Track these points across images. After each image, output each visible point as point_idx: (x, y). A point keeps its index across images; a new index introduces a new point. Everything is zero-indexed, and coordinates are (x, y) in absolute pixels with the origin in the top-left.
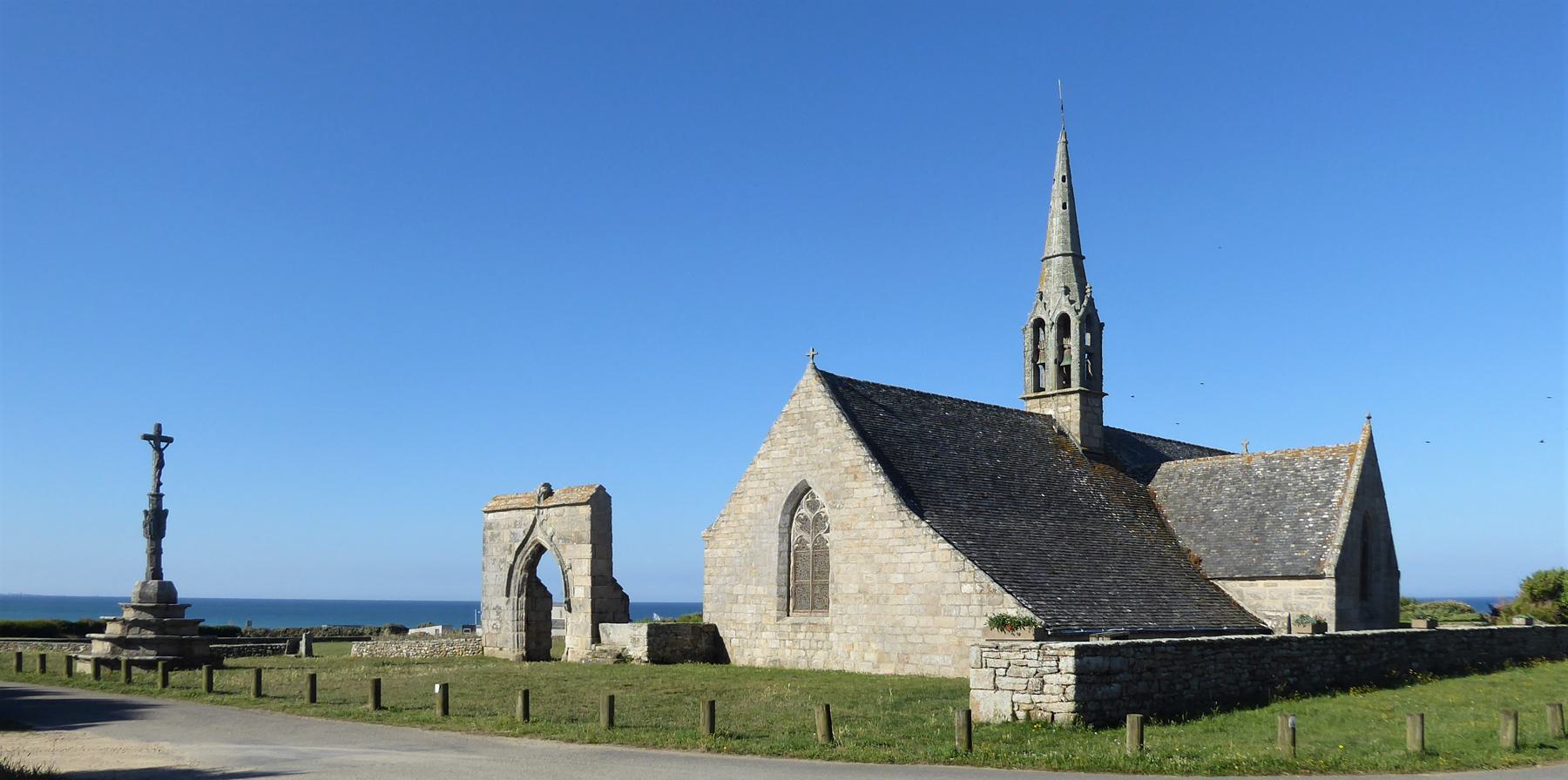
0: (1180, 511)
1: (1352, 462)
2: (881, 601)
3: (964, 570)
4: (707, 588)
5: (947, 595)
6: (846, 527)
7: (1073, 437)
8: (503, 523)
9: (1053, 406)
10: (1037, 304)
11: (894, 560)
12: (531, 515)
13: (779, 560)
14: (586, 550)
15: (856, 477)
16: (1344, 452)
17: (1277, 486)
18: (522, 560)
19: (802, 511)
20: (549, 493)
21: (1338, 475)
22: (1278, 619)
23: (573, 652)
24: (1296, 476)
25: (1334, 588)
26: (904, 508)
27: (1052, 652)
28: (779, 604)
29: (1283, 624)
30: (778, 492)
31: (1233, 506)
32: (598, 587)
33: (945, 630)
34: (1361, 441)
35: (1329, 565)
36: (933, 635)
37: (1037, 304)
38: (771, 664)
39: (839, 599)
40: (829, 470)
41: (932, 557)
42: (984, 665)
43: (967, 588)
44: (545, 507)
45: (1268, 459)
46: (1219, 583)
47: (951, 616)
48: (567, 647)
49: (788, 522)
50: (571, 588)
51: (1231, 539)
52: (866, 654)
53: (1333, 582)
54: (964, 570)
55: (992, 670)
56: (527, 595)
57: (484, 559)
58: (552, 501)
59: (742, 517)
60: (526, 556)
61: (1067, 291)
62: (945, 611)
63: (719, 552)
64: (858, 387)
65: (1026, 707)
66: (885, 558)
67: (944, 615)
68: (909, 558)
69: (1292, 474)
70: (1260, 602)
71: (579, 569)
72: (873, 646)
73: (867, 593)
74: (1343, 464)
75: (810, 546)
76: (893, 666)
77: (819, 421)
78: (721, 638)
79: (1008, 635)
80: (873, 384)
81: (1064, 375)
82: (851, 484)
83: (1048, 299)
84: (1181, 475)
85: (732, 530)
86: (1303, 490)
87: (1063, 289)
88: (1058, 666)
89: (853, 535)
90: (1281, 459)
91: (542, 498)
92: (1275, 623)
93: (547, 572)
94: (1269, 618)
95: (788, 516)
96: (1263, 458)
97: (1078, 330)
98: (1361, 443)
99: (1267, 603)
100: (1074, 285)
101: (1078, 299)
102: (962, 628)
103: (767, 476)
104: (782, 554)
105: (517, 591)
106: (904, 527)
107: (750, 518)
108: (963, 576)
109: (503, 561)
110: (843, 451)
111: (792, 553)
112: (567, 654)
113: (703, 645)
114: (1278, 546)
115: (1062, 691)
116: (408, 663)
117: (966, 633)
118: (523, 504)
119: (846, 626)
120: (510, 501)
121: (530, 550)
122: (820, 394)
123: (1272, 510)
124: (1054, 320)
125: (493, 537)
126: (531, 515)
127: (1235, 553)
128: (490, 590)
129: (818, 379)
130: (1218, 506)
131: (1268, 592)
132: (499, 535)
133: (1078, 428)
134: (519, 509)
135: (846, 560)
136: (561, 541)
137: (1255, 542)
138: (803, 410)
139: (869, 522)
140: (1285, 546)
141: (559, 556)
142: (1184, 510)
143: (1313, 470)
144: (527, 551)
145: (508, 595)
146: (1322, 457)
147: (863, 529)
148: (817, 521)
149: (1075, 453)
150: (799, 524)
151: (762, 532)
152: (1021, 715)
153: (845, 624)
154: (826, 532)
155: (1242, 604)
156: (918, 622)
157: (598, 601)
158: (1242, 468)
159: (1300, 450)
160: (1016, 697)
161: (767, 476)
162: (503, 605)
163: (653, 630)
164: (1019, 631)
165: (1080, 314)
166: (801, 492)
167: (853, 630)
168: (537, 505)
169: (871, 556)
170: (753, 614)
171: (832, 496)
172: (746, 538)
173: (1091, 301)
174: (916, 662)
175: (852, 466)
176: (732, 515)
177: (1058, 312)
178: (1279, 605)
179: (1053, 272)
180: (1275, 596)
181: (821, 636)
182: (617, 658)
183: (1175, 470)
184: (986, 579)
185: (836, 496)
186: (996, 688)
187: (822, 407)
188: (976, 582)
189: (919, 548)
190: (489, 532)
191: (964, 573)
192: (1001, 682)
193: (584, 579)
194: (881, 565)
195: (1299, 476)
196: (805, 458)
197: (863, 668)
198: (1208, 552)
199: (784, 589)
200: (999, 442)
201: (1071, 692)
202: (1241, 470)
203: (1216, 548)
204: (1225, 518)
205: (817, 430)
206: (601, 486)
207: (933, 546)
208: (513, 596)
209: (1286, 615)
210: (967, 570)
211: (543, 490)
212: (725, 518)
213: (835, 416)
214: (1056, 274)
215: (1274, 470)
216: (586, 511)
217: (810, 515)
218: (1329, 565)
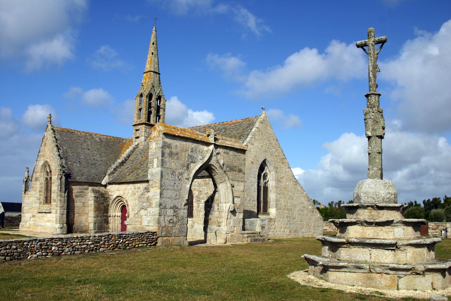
132: (177, 154)
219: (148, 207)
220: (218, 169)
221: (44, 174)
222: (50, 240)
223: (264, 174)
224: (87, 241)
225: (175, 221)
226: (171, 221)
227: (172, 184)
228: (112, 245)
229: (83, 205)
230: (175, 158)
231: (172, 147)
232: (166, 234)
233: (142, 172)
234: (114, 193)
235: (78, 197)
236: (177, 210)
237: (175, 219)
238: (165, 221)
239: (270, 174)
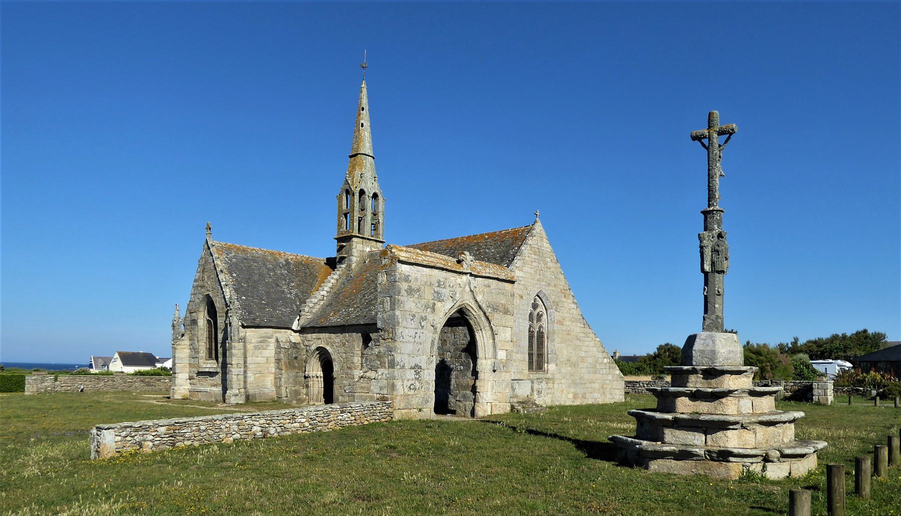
40: (553, 288)
41: (595, 344)
43: (605, 361)
66: (578, 343)
82: (564, 299)
103: (522, 283)
132: (419, 290)
134: (443, 269)
138: (540, 247)
161: (522, 283)
170: (514, 372)
177: (374, 192)
189: (590, 339)
219: (379, 368)
220: (477, 311)
221: (204, 314)
222: (250, 418)
223: (538, 315)
224: (300, 417)
225: (417, 388)
226: (412, 387)
227: (413, 335)
228: (333, 422)
229: (267, 360)
230: (416, 296)
231: (411, 281)
232: (406, 406)
233: (354, 310)
234: (313, 342)
235: (259, 349)
237: (418, 385)
238: (403, 387)
239: (547, 313)
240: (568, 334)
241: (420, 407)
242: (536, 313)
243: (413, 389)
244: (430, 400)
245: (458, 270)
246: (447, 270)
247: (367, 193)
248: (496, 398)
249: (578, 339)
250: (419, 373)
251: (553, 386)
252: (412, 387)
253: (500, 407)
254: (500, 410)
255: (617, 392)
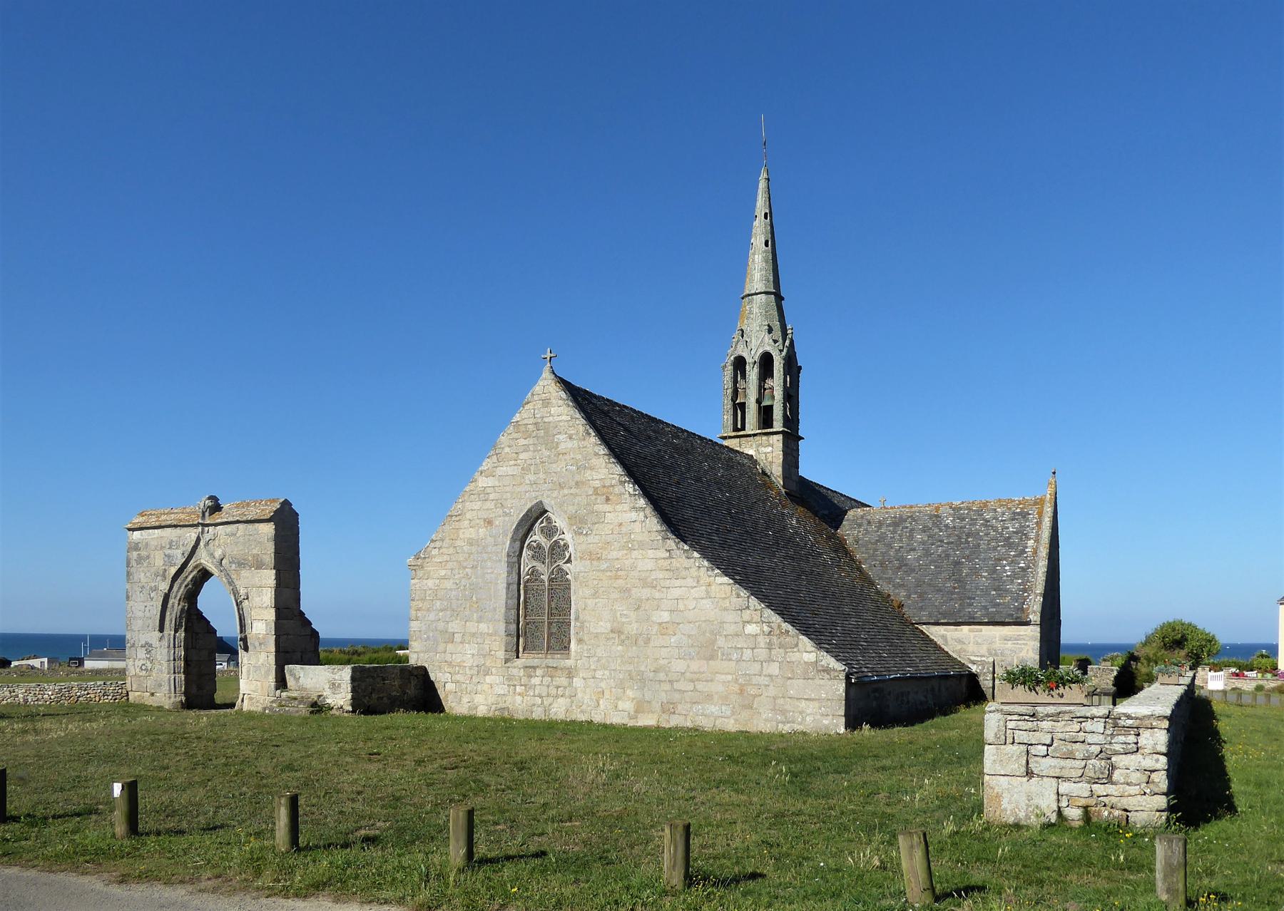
0: (873, 557)
1: (1040, 514)
2: (641, 642)
3: (748, 608)
4: (414, 625)
5: (726, 636)
6: (594, 557)
7: (775, 478)
8: (153, 543)
9: (754, 446)
10: (738, 341)
11: (657, 595)
12: (192, 534)
13: (507, 594)
14: (268, 577)
15: (608, 499)
16: (1030, 505)
17: (968, 535)
18: (180, 588)
19: (534, 538)
20: (216, 508)
21: (1028, 526)
22: (983, 663)
23: (251, 699)
24: (986, 526)
25: (1039, 635)
26: (670, 535)
27: (1130, 722)
28: (507, 644)
29: (988, 669)
30: (506, 514)
31: (927, 553)
32: (285, 622)
33: (723, 677)
34: (1050, 491)
35: (1034, 612)
36: (707, 681)
37: (738, 341)
38: (497, 713)
39: (586, 638)
40: (573, 491)
41: (707, 592)
42: (1009, 740)
43: (751, 629)
44: (211, 525)
45: (957, 509)
46: (923, 628)
47: (731, 660)
48: (241, 692)
49: (518, 550)
50: (248, 622)
51: (929, 585)
52: (620, 702)
53: (1038, 629)
54: (748, 608)
55: (1024, 748)
56: (186, 630)
57: (128, 586)
58: (218, 518)
59: (459, 543)
60: (186, 583)
61: (770, 330)
62: (723, 655)
63: (430, 583)
64: (594, 401)
65: (1083, 802)
66: (646, 593)
67: (722, 660)
68: (676, 593)
69: (982, 524)
70: (964, 646)
71: (257, 599)
72: (630, 693)
73: (622, 633)
74: (1031, 516)
75: (545, 578)
76: (656, 716)
77: (560, 433)
78: (432, 682)
79: (1043, 697)
80: (608, 400)
81: (766, 416)
82: (601, 507)
83: (750, 337)
84: (869, 522)
85: (446, 558)
86: (996, 539)
87: (767, 327)
88: (1137, 743)
89: (604, 566)
90: (969, 509)
91: (207, 514)
92: (980, 667)
93: (212, 603)
94: (974, 663)
95: (518, 544)
96: (951, 507)
97: (782, 370)
98: (1048, 496)
99: (971, 648)
100: (776, 325)
101: (780, 339)
102: (746, 674)
103: (491, 497)
104: (511, 587)
105: (173, 625)
106: (670, 557)
107: (471, 544)
108: (747, 615)
109: (155, 589)
110: (592, 469)
111: (522, 586)
112: (243, 701)
113: (412, 691)
114: (978, 593)
115: (1145, 779)
116: (31, 715)
117: (750, 680)
118: (181, 520)
119: (595, 670)
120: (163, 517)
121: (191, 577)
122: (561, 402)
123: (968, 558)
124: (757, 358)
125: (140, 560)
126: (192, 534)
127: (936, 598)
128: (138, 624)
129: (558, 384)
130: (912, 553)
131: (972, 637)
132: (148, 557)
133: (780, 469)
134: (176, 526)
135: (595, 595)
136: (234, 565)
137: (955, 588)
138: (539, 421)
139: (625, 552)
140: (986, 593)
141: (231, 583)
142: (877, 556)
143: (1002, 521)
144: (186, 577)
145: (161, 629)
146: (1010, 509)
147: (617, 559)
148: (553, 549)
149: (779, 493)
150: (531, 553)
151: (485, 561)
152: (1074, 814)
153: (592, 667)
154: (564, 563)
155: (946, 649)
156: (688, 666)
157: (283, 638)
158: (931, 517)
159: (987, 502)
160: (1065, 787)
161: (491, 497)
162: (155, 642)
163: (358, 674)
164: (1061, 690)
165: (784, 353)
166: (535, 515)
167: (603, 675)
168: (201, 521)
169: (628, 590)
171: (579, 523)
172: (465, 568)
173: (792, 342)
174: (684, 712)
175: (604, 487)
176: (447, 540)
178: (984, 650)
179: (755, 310)
180: (979, 641)
181: (563, 681)
182: (312, 706)
183: (862, 517)
184: (776, 619)
185: (582, 521)
186: (1029, 774)
187: (564, 418)
188: (763, 622)
189: (690, 582)
190: (135, 554)
191: (748, 612)
192: (1040, 765)
193: (265, 612)
194: (641, 600)
195: (989, 526)
196: (542, 476)
197: (616, 719)
198: (908, 597)
199: (514, 627)
200: (722, 476)
201: (1162, 781)
202: (930, 519)
203: (916, 593)
204: (920, 565)
205: (557, 443)
206: (286, 500)
207: (708, 580)
208: (169, 631)
209: (991, 660)
210: (752, 608)
211: (209, 503)
212: (438, 544)
213: (581, 429)
214: (756, 316)
215: (963, 519)
216: (268, 529)
217: (546, 544)
218: (1034, 612)
225: (149, 668)
226: (143, 668)
236: (150, 649)
237: (149, 665)
240: (617, 578)
241: (153, 691)
242: (546, 544)
243: (144, 670)
244: (163, 683)
245: (187, 523)
246: (180, 526)
247: (749, 360)
248: (253, 687)
249: (645, 583)
250: (150, 651)
251: (570, 684)
252: (143, 668)
253: (257, 702)
254: (257, 706)
255: (811, 708)
